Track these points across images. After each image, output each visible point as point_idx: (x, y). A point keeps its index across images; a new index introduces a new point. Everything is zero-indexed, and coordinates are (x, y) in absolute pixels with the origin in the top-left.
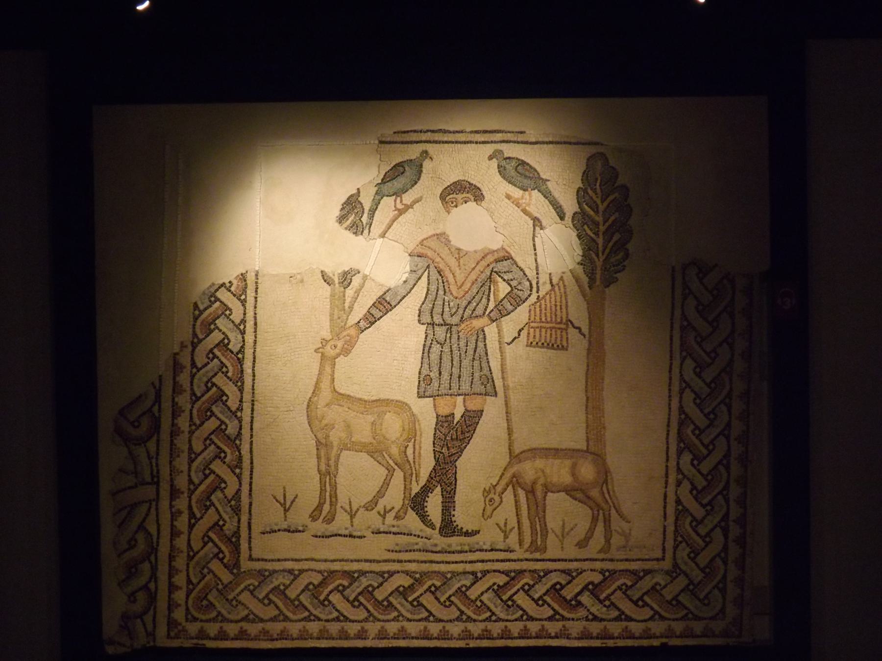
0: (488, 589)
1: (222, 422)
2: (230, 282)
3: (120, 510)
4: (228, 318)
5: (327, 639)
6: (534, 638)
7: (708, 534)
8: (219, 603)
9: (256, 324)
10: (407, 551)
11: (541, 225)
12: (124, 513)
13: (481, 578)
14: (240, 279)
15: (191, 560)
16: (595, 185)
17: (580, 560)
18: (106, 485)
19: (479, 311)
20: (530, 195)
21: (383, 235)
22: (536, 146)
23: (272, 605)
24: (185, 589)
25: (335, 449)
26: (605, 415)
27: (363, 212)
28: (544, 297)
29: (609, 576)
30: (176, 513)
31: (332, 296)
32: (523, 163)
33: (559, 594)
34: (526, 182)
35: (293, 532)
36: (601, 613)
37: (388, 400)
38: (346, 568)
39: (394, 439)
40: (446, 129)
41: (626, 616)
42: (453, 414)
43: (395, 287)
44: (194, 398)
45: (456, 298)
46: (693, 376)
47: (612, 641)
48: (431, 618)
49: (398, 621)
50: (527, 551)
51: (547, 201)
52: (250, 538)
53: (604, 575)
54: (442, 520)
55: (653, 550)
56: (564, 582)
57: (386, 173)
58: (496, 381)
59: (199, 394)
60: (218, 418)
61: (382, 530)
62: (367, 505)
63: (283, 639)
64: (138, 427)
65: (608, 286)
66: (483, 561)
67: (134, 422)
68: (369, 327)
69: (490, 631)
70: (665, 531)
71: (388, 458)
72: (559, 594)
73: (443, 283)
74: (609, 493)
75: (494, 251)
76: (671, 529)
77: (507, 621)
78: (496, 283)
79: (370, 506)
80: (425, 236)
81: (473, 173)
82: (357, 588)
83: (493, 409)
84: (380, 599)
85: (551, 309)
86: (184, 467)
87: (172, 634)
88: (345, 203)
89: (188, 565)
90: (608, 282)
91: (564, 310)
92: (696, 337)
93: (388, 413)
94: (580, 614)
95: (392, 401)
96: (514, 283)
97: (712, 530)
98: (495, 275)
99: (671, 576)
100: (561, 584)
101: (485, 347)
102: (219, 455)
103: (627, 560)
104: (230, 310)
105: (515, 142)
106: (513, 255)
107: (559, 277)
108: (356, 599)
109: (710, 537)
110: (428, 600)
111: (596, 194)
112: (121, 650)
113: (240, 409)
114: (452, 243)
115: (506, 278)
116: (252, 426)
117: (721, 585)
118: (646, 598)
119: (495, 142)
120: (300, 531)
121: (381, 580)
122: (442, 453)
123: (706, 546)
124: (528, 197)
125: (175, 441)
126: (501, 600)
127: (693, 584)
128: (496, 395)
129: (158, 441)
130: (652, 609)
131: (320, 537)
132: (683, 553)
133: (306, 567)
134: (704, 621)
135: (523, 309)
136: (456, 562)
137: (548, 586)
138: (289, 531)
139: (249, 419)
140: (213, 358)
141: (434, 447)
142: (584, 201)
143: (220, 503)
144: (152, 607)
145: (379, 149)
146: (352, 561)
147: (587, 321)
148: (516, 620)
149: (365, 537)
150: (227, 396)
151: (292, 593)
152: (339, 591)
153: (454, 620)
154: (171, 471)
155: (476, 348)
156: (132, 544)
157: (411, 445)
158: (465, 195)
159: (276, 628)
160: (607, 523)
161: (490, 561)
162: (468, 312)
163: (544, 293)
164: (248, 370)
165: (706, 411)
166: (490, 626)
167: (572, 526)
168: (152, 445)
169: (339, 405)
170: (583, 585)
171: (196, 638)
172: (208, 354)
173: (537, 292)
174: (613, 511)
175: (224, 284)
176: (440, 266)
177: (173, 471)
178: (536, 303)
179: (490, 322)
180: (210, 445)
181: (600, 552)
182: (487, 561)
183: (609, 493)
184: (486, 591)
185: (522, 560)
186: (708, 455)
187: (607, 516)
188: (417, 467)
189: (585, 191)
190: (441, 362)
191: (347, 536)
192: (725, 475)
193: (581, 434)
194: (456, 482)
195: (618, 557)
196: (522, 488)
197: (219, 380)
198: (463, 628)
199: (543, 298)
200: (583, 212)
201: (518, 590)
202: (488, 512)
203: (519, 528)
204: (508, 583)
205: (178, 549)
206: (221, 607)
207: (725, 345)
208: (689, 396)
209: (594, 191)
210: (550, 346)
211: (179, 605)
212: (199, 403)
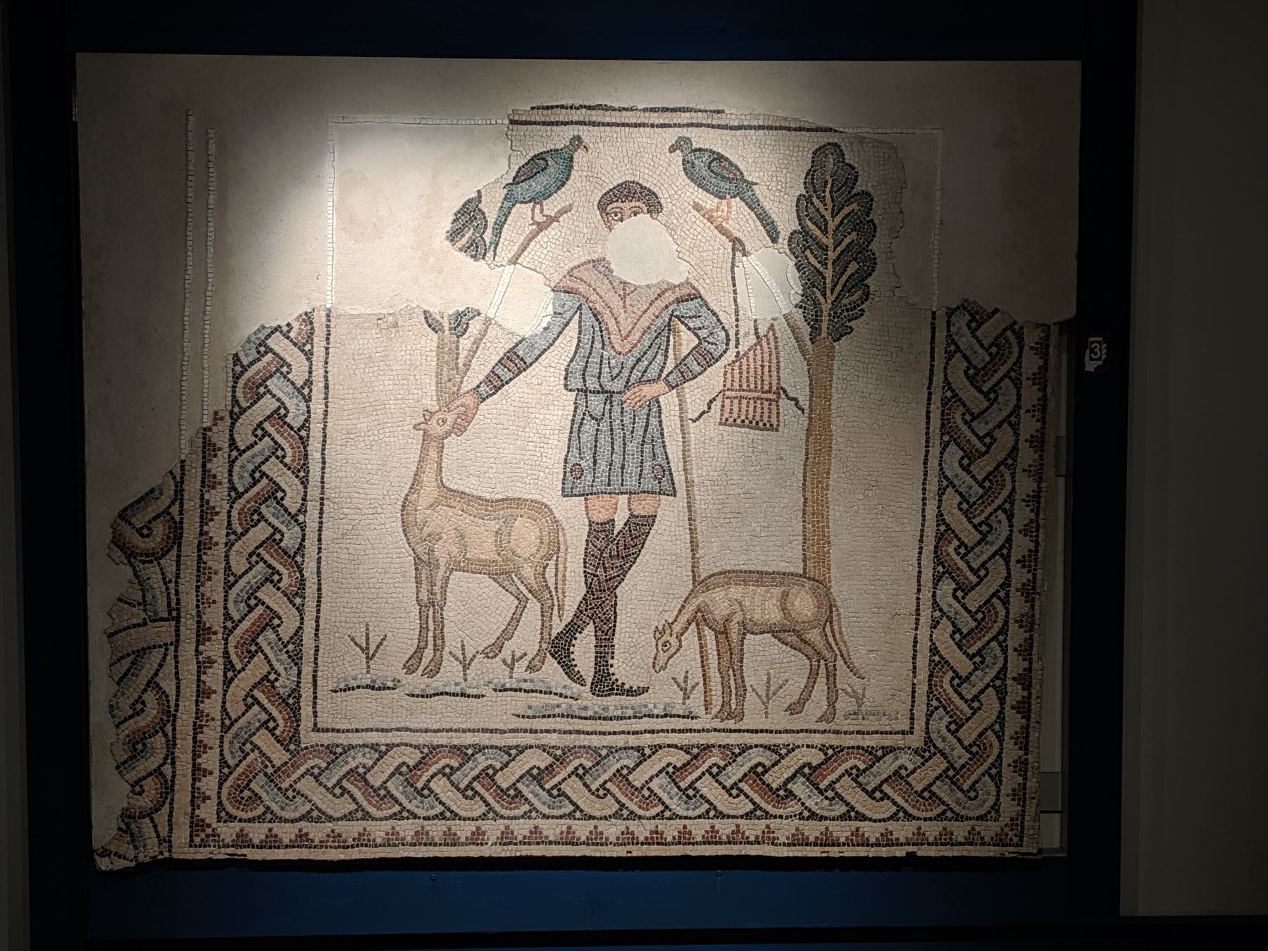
0: (660, 772)
1: (276, 530)
2: (288, 325)
3: (123, 657)
4: (285, 377)
5: (425, 845)
6: (725, 843)
7: (976, 697)
8: (268, 793)
9: (327, 387)
10: (544, 717)
11: (744, 249)
12: (126, 663)
14: (304, 321)
15: (226, 732)
16: (824, 191)
17: (792, 731)
18: (98, 623)
22: (739, 132)
23: (346, 796)
24: (217, 773)
25: (442, 569)
27: (486, 226)
28: (746, 354)
29: (833, 754)
30: (204, 662)
31: (440, 347)
32: (720, 158)
33: (761, 780)
34: (724, 185)
35: (379, 689)
36: (822, 809)
37: (519, 499)
38: (456, 742)
39: (526, 555)
40: (609, 104)
41: (857, 812)
43: (532, 336)
44: (233, 494)
45: (620, 353)
46: (960, 471)
47: (836, 848)
48: (578, 814)
49: (530, 818)
50: (716, 717)
51: (753, 214)
52: (315, 698)
53: (826, 754)
54: (596, 673)
55: (897, 718)
56: (768, 763)
57: (520, 169)
58: (674, 474)
59: (241, 490)
60: (270, 524)
61: (508, 686)
62: (488, 650)
63: (362, 845)
64: (148, 536)
65: (839, 339)
66: (652, 732)
67: (142, 528)
68: (494, 394)
69: (662, 833)
70: (914, 692)
71: (519, 583)
72: (761, 780)
73: (601, 331)
74: (834, 636)
75: (675, 287)
76: (922, 689)
77: (686, 818)
78: (677, 332)
79: (493, 651)
80: (576, 263)
81: (647, 171)
82: (471, 770)
84: (504, 786)
85: (756, 372)
86: (220, 597)
87: (197, 840)
88: (459, 212)
89: (222, 737)
92: (964, 414)
93: (519, 519)
94: (791, 809)
95: (527, 500)
96: (703, 333)
97: (982, 691)
99: (923, 757)
100: (764, 766)
101: (661, 425)
102: (271, 578)
103: (858, 732)
104: (289, 366)
105: (708, 126)
107: (769, 325)
108: (469, 787)
109: (979, 701)
110: (573, 788)
111: (825, 205)
112: (120, 864)
113: (303, 510)
115: (691, 325)
116: (320, 535)
117: (994, 771)
118: (885, 787)
119: (680, 126)
120: (389, 688)
121: (506, 758)
122: (597, 576)
123: (973, 714)
124: (726, 208)
125: (205, 558)
126: (679, 787)
127: (955, 769)
129: (179, 556)
130: (895, 803)
131: (418, 696)
132: (940, 723)
133: (398, 741)
134: (971, 822)
135: (717, 370)
136: (615, 733)
137: (746, 768)
138: (373, 688)
139: (316, 525)
140: (263, 436)
141: (585, 567)
142: (807, 216)
143: (272, 648)
144: (168, 801)
145: (510, 133)
146: (464, 731)
147: (808, 388)
148: (700, 817)
149: (483, 696)
150: (283, 491)
151: (376, 779)
152: (444, 775)
153: (610, 816)
154: (198, 601)
155: (647, 426)
156: (138, 708)
157: (552, 563)
158: (633, 204)
159: (351, 830)
160: (831, 679)
161: (662, 731)
162: (636, 374)
163: (746, 349)
165: (976, 521)
166: (662, 825)
167: (780, 682)
168: (169, 563)
169: (448, 506)
170: (796, 767)
171: (232, 846)
172: (255, 430)
173: (737, 347)
174: (840, 662)
175: (279, 327)
176: (597, 306)
177: (201, 600)
178: (734, 362)
179: (667, 389)
180: (257, 563)
181: (820, 720)
182: (658, 732)
183: (834, 636)
184: (657, 775)
185: (708, 731)
186: (978, 583)
187: (831, 669)
189: (809, 200)
190: (596, 446)
191: (457, 695)
192: (1003, 613)
194: (615, 617)
195: (845, 728)
196: (710, 628)
197: (272, 468)
198: (623, 828)
199: (744, 355)
200: (805, 232)
201: (703, 774)
202: (661, 662)
203: (705, 684)
204: (688, 763)
205: (208, 715)
207: (1005, 425)
208: (951, 499)
209: (823, 200)
211: (209, 798)
212: (242, 501)
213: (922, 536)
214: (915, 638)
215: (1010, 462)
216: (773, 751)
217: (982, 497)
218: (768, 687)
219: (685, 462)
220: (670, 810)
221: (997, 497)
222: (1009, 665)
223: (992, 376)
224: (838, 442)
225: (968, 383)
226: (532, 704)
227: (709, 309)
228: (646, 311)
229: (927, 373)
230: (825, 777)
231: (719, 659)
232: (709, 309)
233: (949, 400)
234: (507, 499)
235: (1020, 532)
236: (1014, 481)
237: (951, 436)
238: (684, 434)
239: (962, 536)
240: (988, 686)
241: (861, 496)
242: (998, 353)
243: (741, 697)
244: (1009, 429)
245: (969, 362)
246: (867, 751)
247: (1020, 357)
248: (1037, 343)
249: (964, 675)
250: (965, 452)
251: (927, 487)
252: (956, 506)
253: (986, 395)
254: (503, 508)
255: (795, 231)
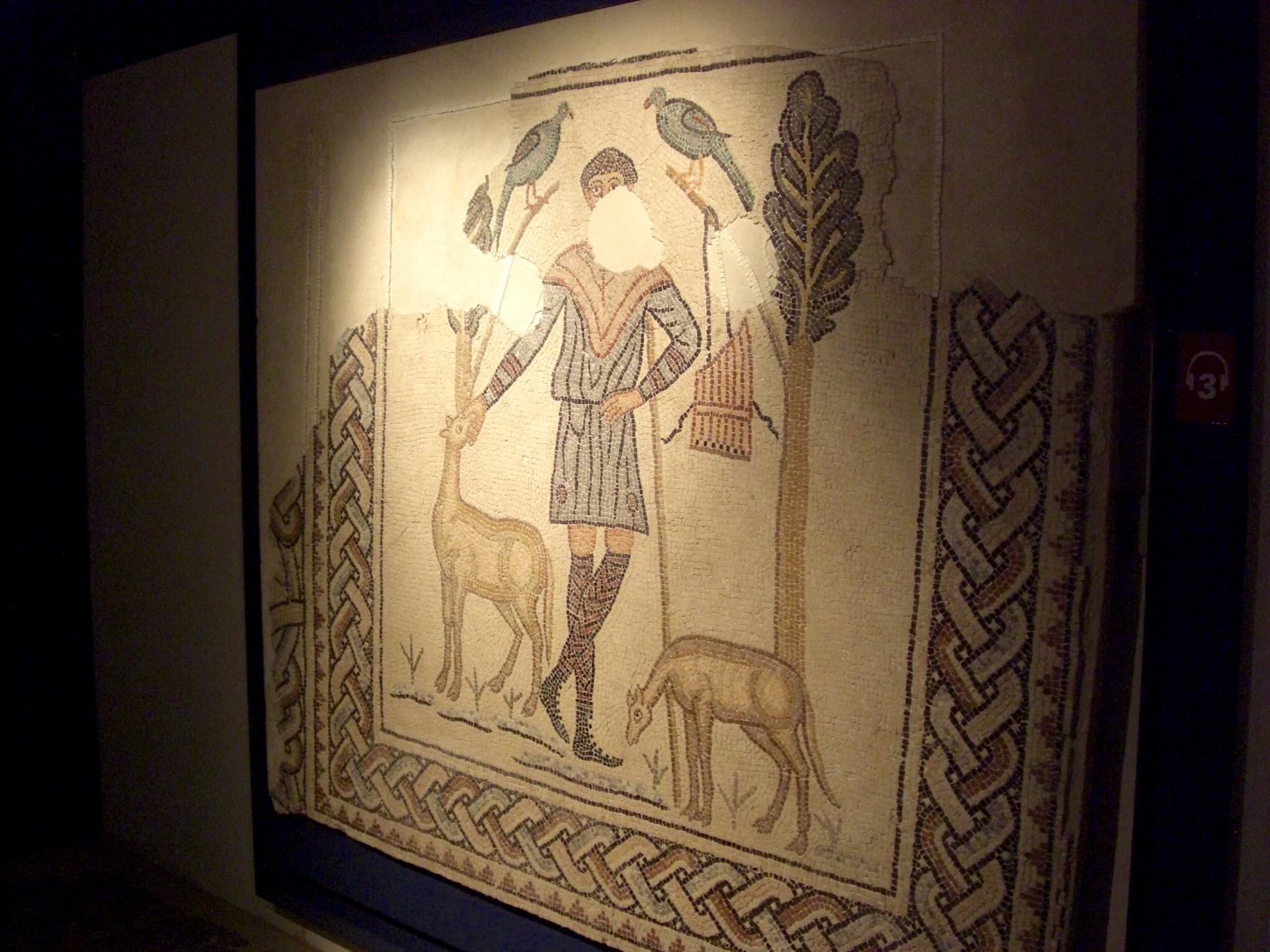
0: (633, 860)
2: (362, 327)
7: (975, 869)
11: (717, 221)
13: (623, 840)
16: (801, 138)
19: (627, 381)
20: (701, 164)
21: (512, 252)
25: (460, 589)
26: (806, 594)
27: (491, 213)
32: (692, 107)
34: (696, 143)
37: (516, 520)
38: (472, 772)
39: (522, 585)
42: (592, 556)
45: (598, 355)
46: (962, 535)
53: (795, 893)
56: (734, 885)
65: (818, 338)
66: (626, 812)
70: (898, 841)
72: (727, 902)
74: (807, 743)
76: (908, 839)
79: (497, 684)
83: (642, 552)
85: (727, 380)
88: (472, 201)
89: (329, 718)
91: (747, 383)
92: (971, 452)
96: (676, 331)
97: (984, 862)
98: (649, 316)
99: (905, 931)
101: (635, 445)
103: (832, 876)
106: (675, 278)
107: (741, 319)
109: (979, 875)
111: (803, 155)
114: (596, 260)
115: (664, 320)
120: (426, 703)
123: (970, 891)
124: (699, 171)
128: (646, 532)
132: (928, 891)
135: (689, 376)
136: (594, 804)
137: (711, 884)
141: (568, 607)
142: (784, 171)
147: (782, 406)
155: (622, 445)
157: (541, 596)
158: (614, 174)
163: (718, 350)
164: (378, 458)
165: (984, 613)
174: (813, 780)
183: (807, 743)
185: (677, 827)
186: (984, 707)
187: (802, 785)
188: (548, 635)
189: (785, 151)
192: (1015, 756)
193: (767, 625)
194: (593, 671)
196: (679, 703)
202: (633, 734)
203: (674, 771)
206: (359, 787)
207: (1027, 472)
208: (952, 578)
209: (799, 148)
213: (914, 625)
214: (902, 767)
215: (1032, 529)
216: (740, 871)
217: (992, 578)
218: (736, 792)
219: (657, 493)
220: (641, 907)
221: (1012, 582)
222: (1022, 833)
223: (1011, 395)
224: (816, 482)
225: (977, 405)
226: (529, 751)
227: (681, 300)
228: (622, 304)
229: (925, 388)
230: (793, 921)
231: (688, 743)
232: (681, 300)
233: (952, 430)
234: (507, 520)
235: (1043, 638)
236: (1036, 560)
237: (954, 484)
238: (656, 457)
239: (964, 632)
240: (990, 857)
241: (841, 559)
242: (1019, 360)
243: (710, 793)
244: (1032, 479)
245: (979, 374)
246: (840, 903)
247: (1049, 368)
248: (1074, 346)
249: (961, 831)
250: (971, 508)
251: (922, 555)
252: (956, 587)
253: (1001, 424)
254: (504, 529)
255: (771, 193)
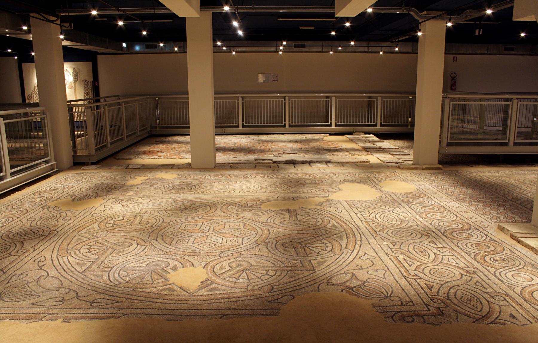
90: (76, 82)
210: (71, 89)
